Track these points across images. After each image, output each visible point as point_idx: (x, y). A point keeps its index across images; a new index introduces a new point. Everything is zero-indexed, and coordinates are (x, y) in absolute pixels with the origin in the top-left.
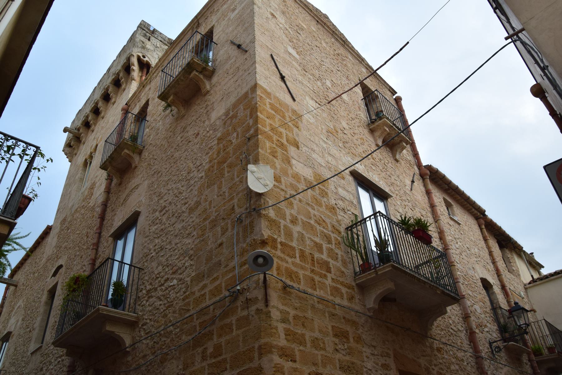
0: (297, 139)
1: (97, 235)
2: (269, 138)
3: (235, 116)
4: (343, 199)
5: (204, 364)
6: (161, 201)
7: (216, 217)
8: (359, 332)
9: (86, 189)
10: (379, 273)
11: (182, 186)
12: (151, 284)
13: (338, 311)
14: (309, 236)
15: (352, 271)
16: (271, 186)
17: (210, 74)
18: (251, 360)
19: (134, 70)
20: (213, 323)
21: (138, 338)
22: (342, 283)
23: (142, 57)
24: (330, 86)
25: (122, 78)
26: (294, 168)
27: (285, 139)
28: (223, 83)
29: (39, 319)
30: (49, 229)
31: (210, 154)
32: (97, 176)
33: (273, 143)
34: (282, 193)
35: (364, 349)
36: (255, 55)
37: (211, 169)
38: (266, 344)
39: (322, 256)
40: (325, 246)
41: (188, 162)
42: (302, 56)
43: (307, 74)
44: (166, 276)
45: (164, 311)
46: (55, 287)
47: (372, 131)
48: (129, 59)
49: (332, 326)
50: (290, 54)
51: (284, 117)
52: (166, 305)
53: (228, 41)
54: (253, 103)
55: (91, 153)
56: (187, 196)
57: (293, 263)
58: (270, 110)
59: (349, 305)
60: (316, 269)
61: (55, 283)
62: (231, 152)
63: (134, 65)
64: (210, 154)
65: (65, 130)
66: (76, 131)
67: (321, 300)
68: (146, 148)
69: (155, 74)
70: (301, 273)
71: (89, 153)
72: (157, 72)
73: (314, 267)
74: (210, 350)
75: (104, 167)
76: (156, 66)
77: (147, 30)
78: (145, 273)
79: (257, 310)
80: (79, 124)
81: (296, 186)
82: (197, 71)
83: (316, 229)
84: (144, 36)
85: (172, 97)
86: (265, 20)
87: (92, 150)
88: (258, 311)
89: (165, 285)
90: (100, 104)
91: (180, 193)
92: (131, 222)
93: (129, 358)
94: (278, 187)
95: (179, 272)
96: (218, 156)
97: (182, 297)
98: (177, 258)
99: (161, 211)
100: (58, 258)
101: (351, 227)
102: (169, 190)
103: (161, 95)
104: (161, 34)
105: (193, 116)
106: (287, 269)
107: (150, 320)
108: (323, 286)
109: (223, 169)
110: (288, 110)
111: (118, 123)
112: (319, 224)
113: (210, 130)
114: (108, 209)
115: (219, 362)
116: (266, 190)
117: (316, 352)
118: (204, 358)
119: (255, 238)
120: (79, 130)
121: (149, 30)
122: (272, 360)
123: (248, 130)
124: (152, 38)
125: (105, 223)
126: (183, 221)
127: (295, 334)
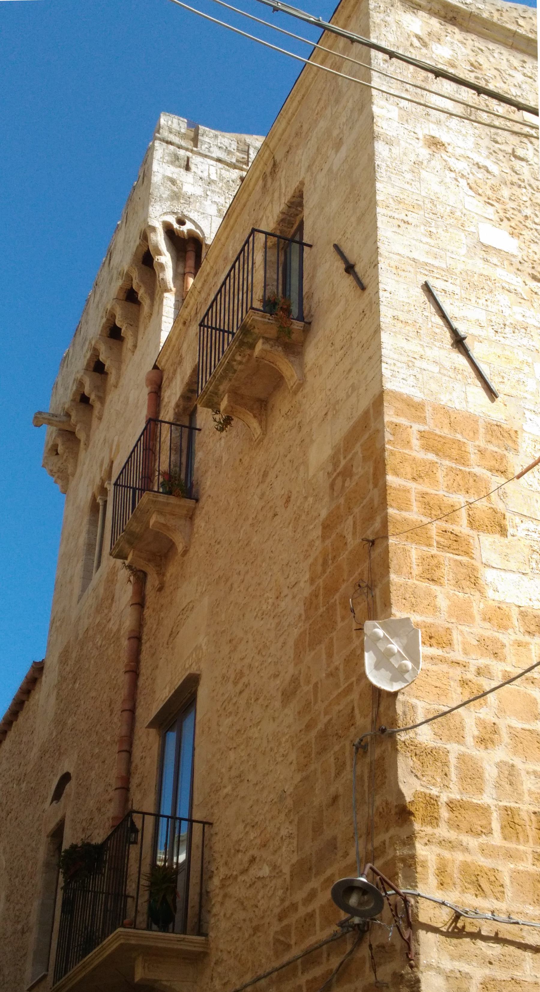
0: (500, 507)
1: (126, 714)
3: (347, 473)
23: (176, 226)
26: (490, 593)
27: (464, 521)
30: (38, 668)
33: (430, 545)
34: (456, 673)
48: (145, 237)
50: (486, 248)
51: (462, 459)
61: (59, 818)
65: (39, 419)
70: (506, 869)
71: (98, 481)
81: (495, 641)
84: (172, 163)
86: (409, 176)
94: (443, 660)
96: (324, 571)
106: (465, 868)
110: (475, 432)
114: (144, 648)
123: (369, 519)
124: (195, 160)
125: (141, 681)
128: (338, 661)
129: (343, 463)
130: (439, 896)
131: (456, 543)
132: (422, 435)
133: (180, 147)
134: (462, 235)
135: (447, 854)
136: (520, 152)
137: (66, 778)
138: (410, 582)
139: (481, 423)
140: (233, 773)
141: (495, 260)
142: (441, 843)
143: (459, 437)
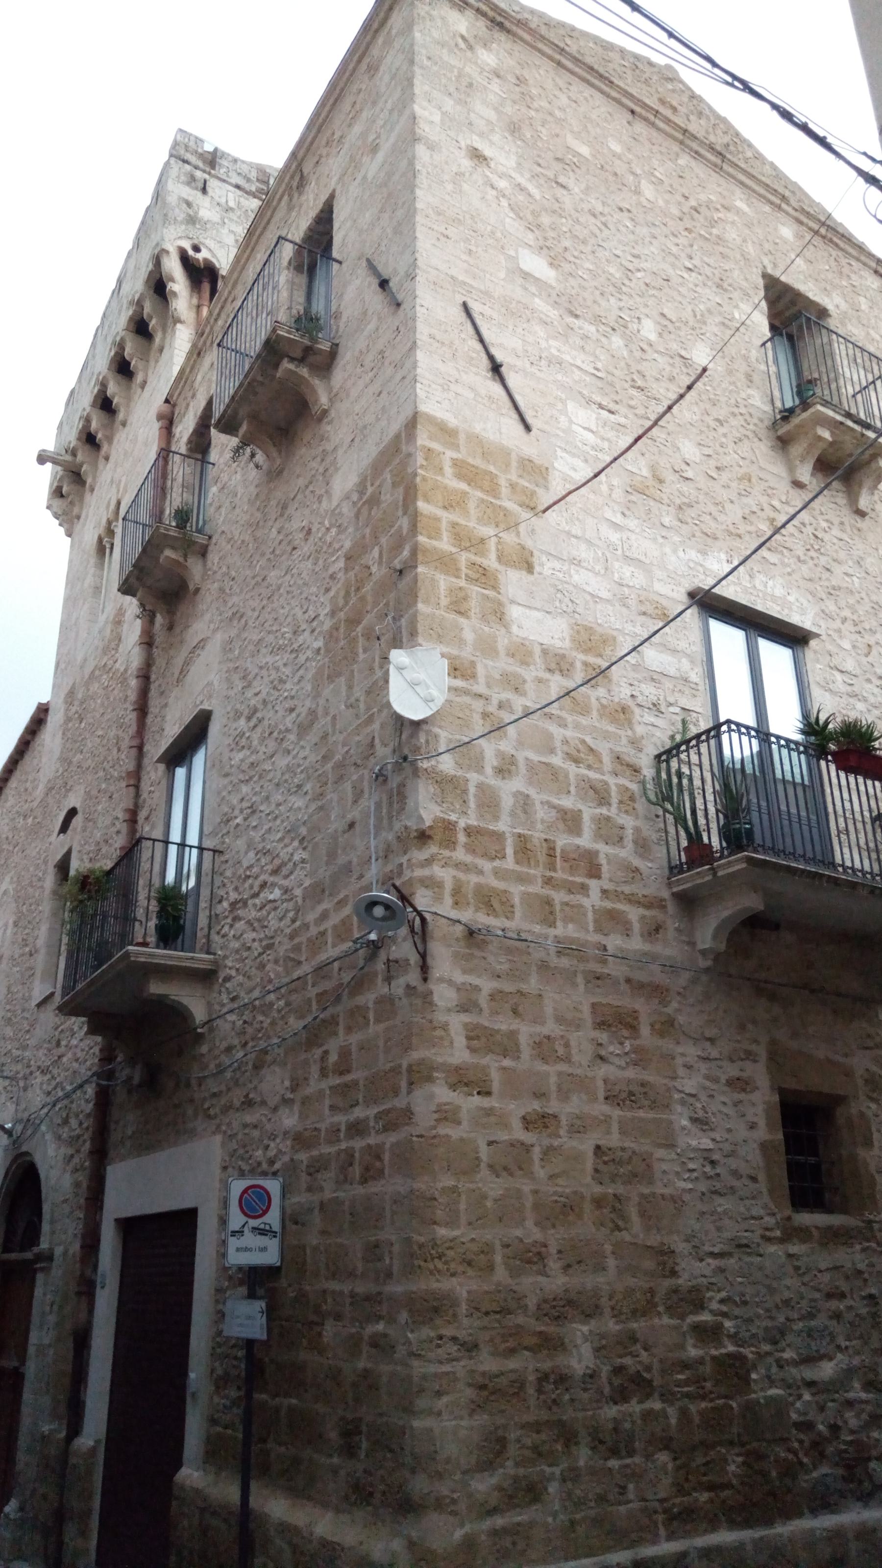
0: (529, 543)
1: (134, 751)
2: (447, 563)
3: (374, 501)
5: (324, 1085)
6: (249, 693)
7: (344, 758)
8: (669, 1010)
10: (720, 874)
12: (236, 889)
13: (615, 969)
14: (545, 797)
15: (666, 864)
16: (440, 697)
17: (325, 362)
18: (396, 1092)
19: (175, 294)
20: (338, 999)
21: (217, 1007)
22: (631, 899)
23: (191, 252)
25: (151, 318)
26: (514, 629)
27: (493, 556)
28: (354, 393)
31: (332, 593)
33: (458, 577)
34: (478, 705)
35: (680, 1049)
36: (414, 320)
37: (335, 634)
38: (421, 1062)
39: (578, 841)
40: (589, 813)
41: (294, 603)
42: (567, 267)
45: (260, 954)
47: (783, 443)
48: (157, 262)
49: (593, 1005)
51: (494, 491)
52: (264, 943)
54: (410, 470)
56: (293, 693)
57: (496, 872)
59: (647, 947)
60: (559, 875)
62: (369, 598)
65: (42, 459)
66: (68, 458)
67: (565, 948)
68: (214, 540)
70: (516, 891)
73: (555, 870)
74: (333, 1058)
76: (232, 270)
77: (193, 159)
79: (408, 986)
80: (72, 437)
81: (516, 676)
82: (292, 359)
83: (567, 776)
84: (188, 184)
86: (450, 187)
87: (111, 516)
88: (410, 989)
89: (262, 895)
90: (112, 389)
91: (282, 681)
92: (196, 734)
93: (204, 1049)
94: (466, 692)
95: (285, 871)
97: (288, 931)
98: (281, 840)
100: (67, 789)
101: (668, 752)
102: (261, 668)
104: (235, 161)
108: (574, 913)
109: (355, 639)
110: (508, 465)
111: (153, 456)
112: (577, 761)
113: (332, 526)
115: (346, 1085)
117: (545, 1068)
118: (324, 1073)
119: (409, 824)
120: (74, 454)
122: (432, 1096)
123: (397, 547)
124: (213, 184)
125: (149, 719)
127: (491, 1033)
128: (358, 693)
129: (370, 490)
130: (454, 914)
131: (484, 576)
132: (455, 463)
133: (196, 168)
134: (502, 258)
135: (461, 876)
136: (562, 179)
137: (72, 812)
138: (437, 612)
139: (514, 456)
140: (245, 804)
141: (533, 289)
142: (458, 865)
143: (491, 468)
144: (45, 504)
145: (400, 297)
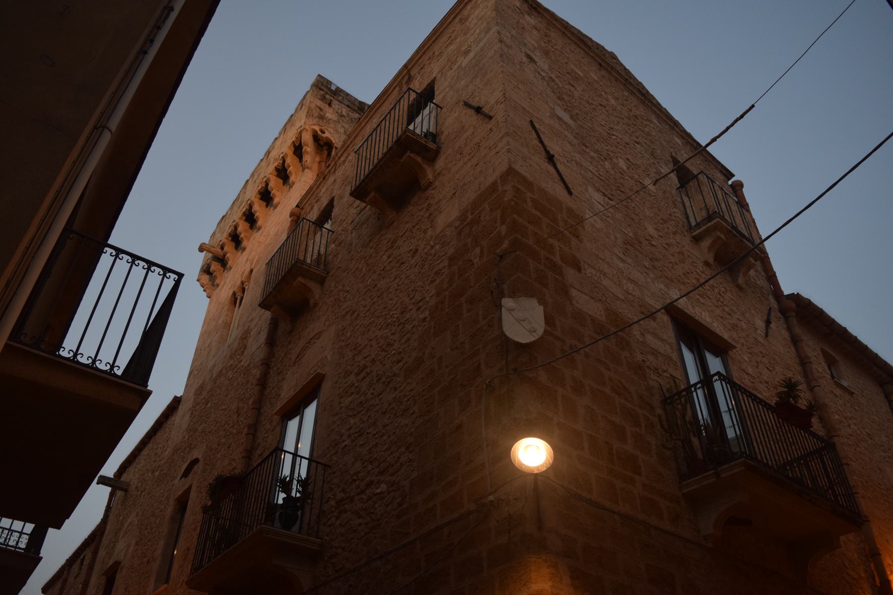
4: (655, 353)
9: (235, 340)
10: (723, 476)
11: (393, 334)
12: (343, 490)
16: (540, 331)
17: (431, 156)
19: (307, 153)
23: (319, 133)
24: (625, 168)
29: (162, 543)
31: (436, 283)
32: (252, 320)
43: (588, 150)
44: (369, 478)
46: (188, 491)
50: (560, 119)
53: (459, 102)
55: (242, 283)
58: (533, 211)
61: (187, 487)
63: (307, 145)
64: (436, 283)
69: (342, 159)
71: (239, 283)
72: (345, 155)
75: (264, 305)
78: (334, 473)
84: (322, 100)
85: (373, 194)
86: (518, 67)
89: (367, 491)
91: (389, 345)
99: (358, 374)
102: (371, 340)
103: (355, 190)
105: (407, 223)
107: (343, 548)
116: (533, 339)
120: (222, 248)
121: (330, 89)
124: (335, 102)
126: (396, 389)
132: (533, 200)
144: (196, 278)
145: (491, 114)
